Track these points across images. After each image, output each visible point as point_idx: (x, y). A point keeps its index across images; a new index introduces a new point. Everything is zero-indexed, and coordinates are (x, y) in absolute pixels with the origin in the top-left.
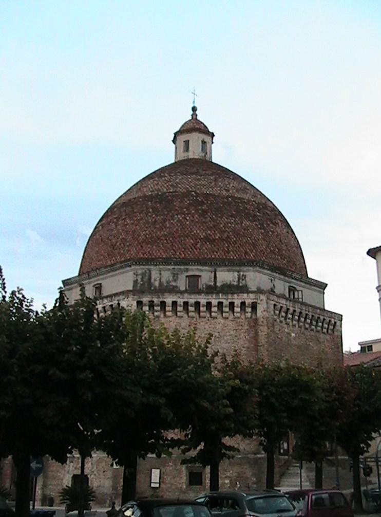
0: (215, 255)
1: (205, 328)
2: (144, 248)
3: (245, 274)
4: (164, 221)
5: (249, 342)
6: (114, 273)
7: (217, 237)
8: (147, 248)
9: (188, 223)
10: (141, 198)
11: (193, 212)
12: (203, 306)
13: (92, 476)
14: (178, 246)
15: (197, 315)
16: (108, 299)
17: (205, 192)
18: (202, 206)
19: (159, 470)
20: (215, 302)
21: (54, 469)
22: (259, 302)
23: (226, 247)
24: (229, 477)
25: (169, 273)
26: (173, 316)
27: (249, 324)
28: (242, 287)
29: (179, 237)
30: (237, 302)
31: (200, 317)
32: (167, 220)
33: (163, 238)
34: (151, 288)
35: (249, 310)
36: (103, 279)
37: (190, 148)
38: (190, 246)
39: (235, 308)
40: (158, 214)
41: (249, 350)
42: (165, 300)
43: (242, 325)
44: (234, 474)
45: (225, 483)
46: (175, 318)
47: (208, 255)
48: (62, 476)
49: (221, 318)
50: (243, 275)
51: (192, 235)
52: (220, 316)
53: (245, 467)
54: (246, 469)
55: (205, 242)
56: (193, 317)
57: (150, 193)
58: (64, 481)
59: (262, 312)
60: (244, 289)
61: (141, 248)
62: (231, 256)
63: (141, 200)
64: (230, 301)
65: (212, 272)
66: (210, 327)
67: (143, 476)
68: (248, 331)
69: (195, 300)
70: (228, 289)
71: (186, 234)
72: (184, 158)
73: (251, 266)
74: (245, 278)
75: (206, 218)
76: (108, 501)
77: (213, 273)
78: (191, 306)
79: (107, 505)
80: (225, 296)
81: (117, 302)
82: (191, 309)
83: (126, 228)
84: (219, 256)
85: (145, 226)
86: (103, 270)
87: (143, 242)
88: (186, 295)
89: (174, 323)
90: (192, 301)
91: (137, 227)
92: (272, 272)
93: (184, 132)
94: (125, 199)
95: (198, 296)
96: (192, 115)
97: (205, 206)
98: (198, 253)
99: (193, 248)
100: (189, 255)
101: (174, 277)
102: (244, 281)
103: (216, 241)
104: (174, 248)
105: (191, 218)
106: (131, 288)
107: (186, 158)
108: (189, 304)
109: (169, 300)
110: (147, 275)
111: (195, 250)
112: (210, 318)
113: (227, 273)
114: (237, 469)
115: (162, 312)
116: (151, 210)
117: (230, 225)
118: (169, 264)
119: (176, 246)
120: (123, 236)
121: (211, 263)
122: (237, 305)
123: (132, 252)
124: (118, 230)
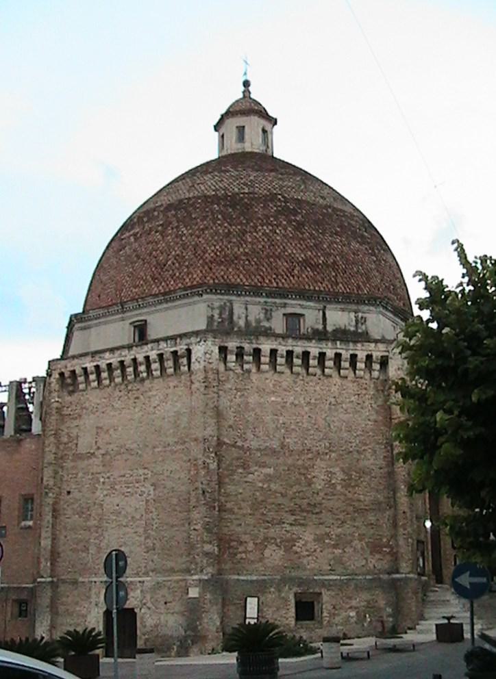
0: (319, 287)
1: (315, 391)
2: (214, 271)
3: (365, 315)
4: (244, 232)
5: (377, 412)
6: (170, 304)
7: (321, 262)
8: (220, 271)
9: (278, 238)
10: (199, 199)
11: (285, 223)
12: (314, 358)
13: (143, 611)
14: (266, 269)
15: (304, 371)
16: (169, 342)
17: (295, 197)
18: (295, 215)
19: (256, 599)
20: (332, 353)
21: (70, 599)
22: (391, 355)
23: (333, 277)
24: (356, 608)
25: (259, 307)
26: (270, 370)
27: (376, 388)
28: (361, 334)
29: (268, 257)
30: (361, 355)
31: (308, 374)
32: (246, 232)
33: (244, 258)
34: (233, 329)
35: (376, 366)
36: (149, 313)
37: (246, 137)
38: (283, 271)
39: (358, 364)
40: (232, 224)
41: (376, 424)
42: (260, 347)
43: (366, 389)
44: (362, 604)
45: (349, 616)
46: (273, 375)
47: (309, 286)
48: (84, 612)
49: (338, 376)
50: (362, 318)
51: (286, 256)
52: (335, 374)
53: (377, 592)
54: (378, 594)
55: (306, 268)
56: (298, 374)
57: (214, 193)
58: (88, 620)
59: (395, 370)
60: (364, 337)
61: (208, 270)
62: (341, 288)
63: (199, 201)
64: (351, 352)
65: (319, 310)
66: (323, 390)
67: (232, 608)
68: (374, 397)
69: (304, 350)
70: (341, 335)
71: (277, 253)
72: (236, 151)
73: (373, 305)
74: (365, 321)
75: (303, 233)
76: (175, 647)
77: (321, 312)
78: (297, 357)
79: (173, 654)
80: (345, 344)
81: (186, 347)
82: (297, 361)
83: (182, 240)
84: (324, 288)
85: (213, 238)
86: (151, 300)
87: (212, 263)
88: (290, 341)
89: (271, 381)
90: (298, 350)
91: (200, 239)
92: (395, 315)
93: (237, 114)
94: (165, 200)
95: (307, 344)
96: (244, 92)
97: (300, 216)
98: (296, 282)
99: (289, 275)
100: (283, 284)
101: (266, 314)
102: (364, 327)
103: (320, 267)
104: (262, 274)
105: (283, 231)
106: (204, 327)
107: (240, 151)
108: (294, 354)
109: (266, 346)
110: (227, 308)
111: (292, 278)
112: (321, 377)
113: (340, 313)
114: (365, 596)
115: (254, 365)
116: (220, 216)
117: (335, 246)
118: (259, 295)
119: (264, 270)
120: (178, 252)
121: (318, 298)
122: (362, 359)
123: (195, 276)
124: (168, 244)
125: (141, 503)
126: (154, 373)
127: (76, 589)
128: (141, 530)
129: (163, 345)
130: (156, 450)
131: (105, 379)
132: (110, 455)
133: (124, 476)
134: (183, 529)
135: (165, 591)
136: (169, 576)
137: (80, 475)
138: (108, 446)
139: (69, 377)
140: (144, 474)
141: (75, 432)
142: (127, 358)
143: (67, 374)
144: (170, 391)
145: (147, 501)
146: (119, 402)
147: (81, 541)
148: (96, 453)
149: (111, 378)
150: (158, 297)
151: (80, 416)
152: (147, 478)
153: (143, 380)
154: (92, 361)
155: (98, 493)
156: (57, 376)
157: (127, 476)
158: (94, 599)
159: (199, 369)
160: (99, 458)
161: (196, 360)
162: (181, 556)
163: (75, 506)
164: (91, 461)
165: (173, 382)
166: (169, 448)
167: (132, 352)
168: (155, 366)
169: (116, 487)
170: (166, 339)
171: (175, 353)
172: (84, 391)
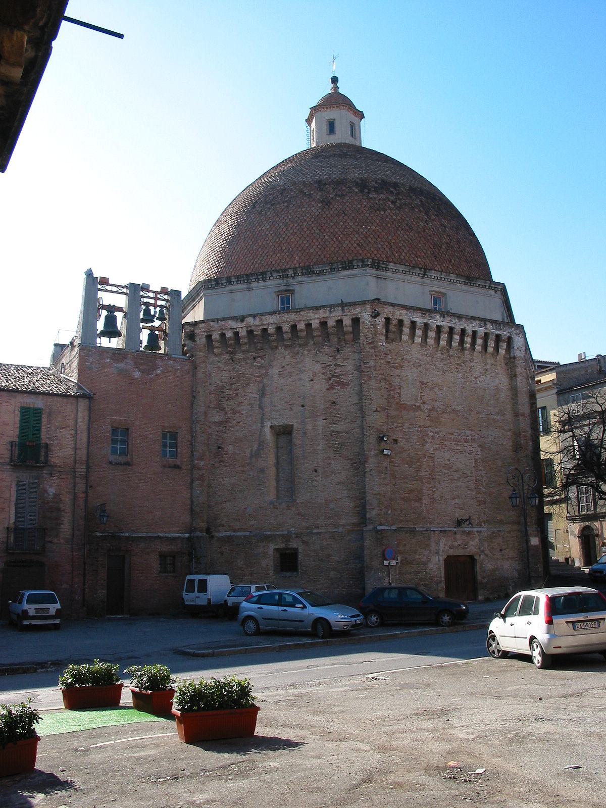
128: (472, 486)
129: (489, 326)
130: (481, 416)
132: (437, 411)
133: (452, 434)
135: (500, 539)
137: (407, 425)
138: (434, 403)
139: (395, 325)
141: (397, 380)
144: (488, 367)
145: (476, 460)
147: (412, 491)
148: (422, 408)
149: (438, 339)
151: (401, 366)
152: (474, 439)
156: (384, 320)
157: (455, 434)
158: (433, 547)
160: (424, 412)
163: (405, 455)
164: (417, 414)
167: (462, 323)
169: (445, 443)
171: (498, 336)
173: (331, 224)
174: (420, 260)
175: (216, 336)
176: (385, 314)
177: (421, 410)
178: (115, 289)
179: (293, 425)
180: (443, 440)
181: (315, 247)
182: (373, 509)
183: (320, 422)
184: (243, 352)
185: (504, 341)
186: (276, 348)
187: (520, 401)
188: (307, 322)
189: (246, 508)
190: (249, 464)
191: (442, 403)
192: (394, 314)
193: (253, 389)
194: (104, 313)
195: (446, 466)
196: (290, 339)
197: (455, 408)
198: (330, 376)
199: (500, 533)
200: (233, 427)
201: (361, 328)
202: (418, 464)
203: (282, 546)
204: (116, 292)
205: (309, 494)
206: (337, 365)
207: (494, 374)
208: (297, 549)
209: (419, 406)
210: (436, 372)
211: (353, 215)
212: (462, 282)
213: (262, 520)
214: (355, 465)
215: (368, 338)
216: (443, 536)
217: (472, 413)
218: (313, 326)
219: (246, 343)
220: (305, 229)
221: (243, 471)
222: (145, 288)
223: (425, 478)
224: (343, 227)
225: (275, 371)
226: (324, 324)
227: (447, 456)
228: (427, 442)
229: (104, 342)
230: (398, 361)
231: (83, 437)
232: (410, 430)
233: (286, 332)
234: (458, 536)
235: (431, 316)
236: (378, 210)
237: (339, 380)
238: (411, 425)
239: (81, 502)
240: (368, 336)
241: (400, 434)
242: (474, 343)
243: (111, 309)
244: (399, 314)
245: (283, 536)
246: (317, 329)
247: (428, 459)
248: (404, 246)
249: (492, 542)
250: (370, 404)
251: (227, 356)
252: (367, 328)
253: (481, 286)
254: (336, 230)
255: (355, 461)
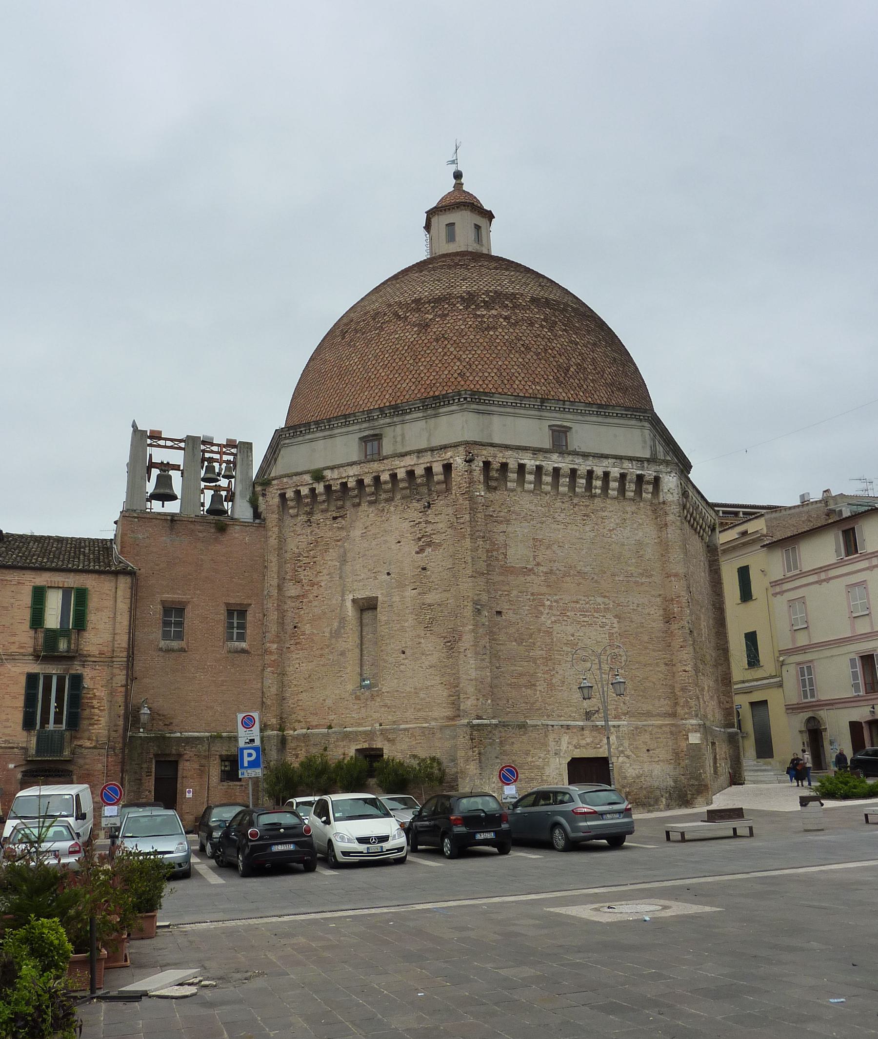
13: (621, 759)
16: (634, 463)
48: (539, 763)
76: (664, 800)
79: (662, 807)
81: (654, 474)
125: (603, 636)
126: (609, 491)
127: (525, 734)
129: (627, 464)
130: (617, 578)
131: (547, 484)
132: (555, 574)
133: (577, 602)
134: (657, 669)
135: (647, 736)
136: (645, 720)
137: (515, 593)
139: (497, 470)
140: (603, 603)
141: (501, 538)
142: (581, 468)
143: (496, 465)
144: (628, 516)
146: (562, 515)
147: (521, 675)
149: (556, 484)
150: (592, 408)
152: (608, 609)
153: (593, 496)
154: (533, 459)
155: (543, 618)
156: (481, 464)
158: (552, 745)
159: (673, 501)
161: (668, 491)
162: (659, 698)
163: (512, 630)
164: (529, 578)
165: (630, 508)
166: (633, 579)
168: (614, 485)
169: (567, 614)
170: (631, 459)
171: (640, 478)
172: (513, 490)
173: (428, 352)
174: (538, 388)
175: (290, 494)
176: (483, 457)
177: (534, 574)
178: (169, 443)
179: (377, 597)
180: (564, 610)
181: (407, 381)
182: (468, 698)
183: (409, 593)
184: (322, 511)
185: (648, 483)
186: (359, 504)
187: (672, 558)
188: (391, 472)
189: (324, 700)
190: (328, 646)
191: (563, 564)
192: (495, 457)
193: (333, 554)
194: (155, 472)
195: (569, 642)
196: (373, 493)
197: (580, 570)
198: (420, 536)
199: (646, 728)
200: (310, 602)
201: (453, 476)
202: (531, 640)
203: (366, 745)
204: (171, 447)
205: (396, 681)
206: (427, 522)
207: (635, 526)
208: (381, 750)
209: (531, 570)
210: (554, 526)
211: (455, 338)
212: (593, 411)
213: (342, 714)
214: (450, 644)
215: (461, 487)
216: (565, 733)
217: (604, 575)
218: (399, 477)
219: (324, 501)
220: (397, 360)
221: (321, 655)
222: (208, 442)
223: (540, 658)
224: (442, 354)
225: (356, 533)
226: (411, 474)
227: (570, 629)
228: (542, 613)
229: (156, 506)
230: (502, 514)
231: (123, 621)
232: (519, 599)
233: (369, 486)
234: (586, 732)
235: (545, 457)
236: (486, 329)
237: (431, 541)
238: (521, 593)
239: (120, 699)
240: (461, 485)
241: (505, 603)
242: (605, 487)
243: (165, 467)
244: (500, 457)
245: (365, 732)
246: (402, 480)
247: (543, 634)
248: (518, 372)
249: (635, 740)
250: (464, 568)
251: (304, 518)
252: (460, 476)
253: (619, 415)
254: (433, 358)
255: (448, 640)
